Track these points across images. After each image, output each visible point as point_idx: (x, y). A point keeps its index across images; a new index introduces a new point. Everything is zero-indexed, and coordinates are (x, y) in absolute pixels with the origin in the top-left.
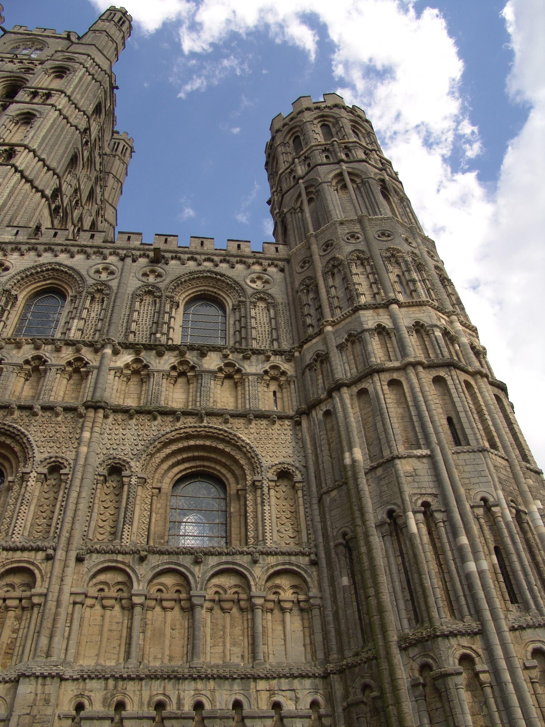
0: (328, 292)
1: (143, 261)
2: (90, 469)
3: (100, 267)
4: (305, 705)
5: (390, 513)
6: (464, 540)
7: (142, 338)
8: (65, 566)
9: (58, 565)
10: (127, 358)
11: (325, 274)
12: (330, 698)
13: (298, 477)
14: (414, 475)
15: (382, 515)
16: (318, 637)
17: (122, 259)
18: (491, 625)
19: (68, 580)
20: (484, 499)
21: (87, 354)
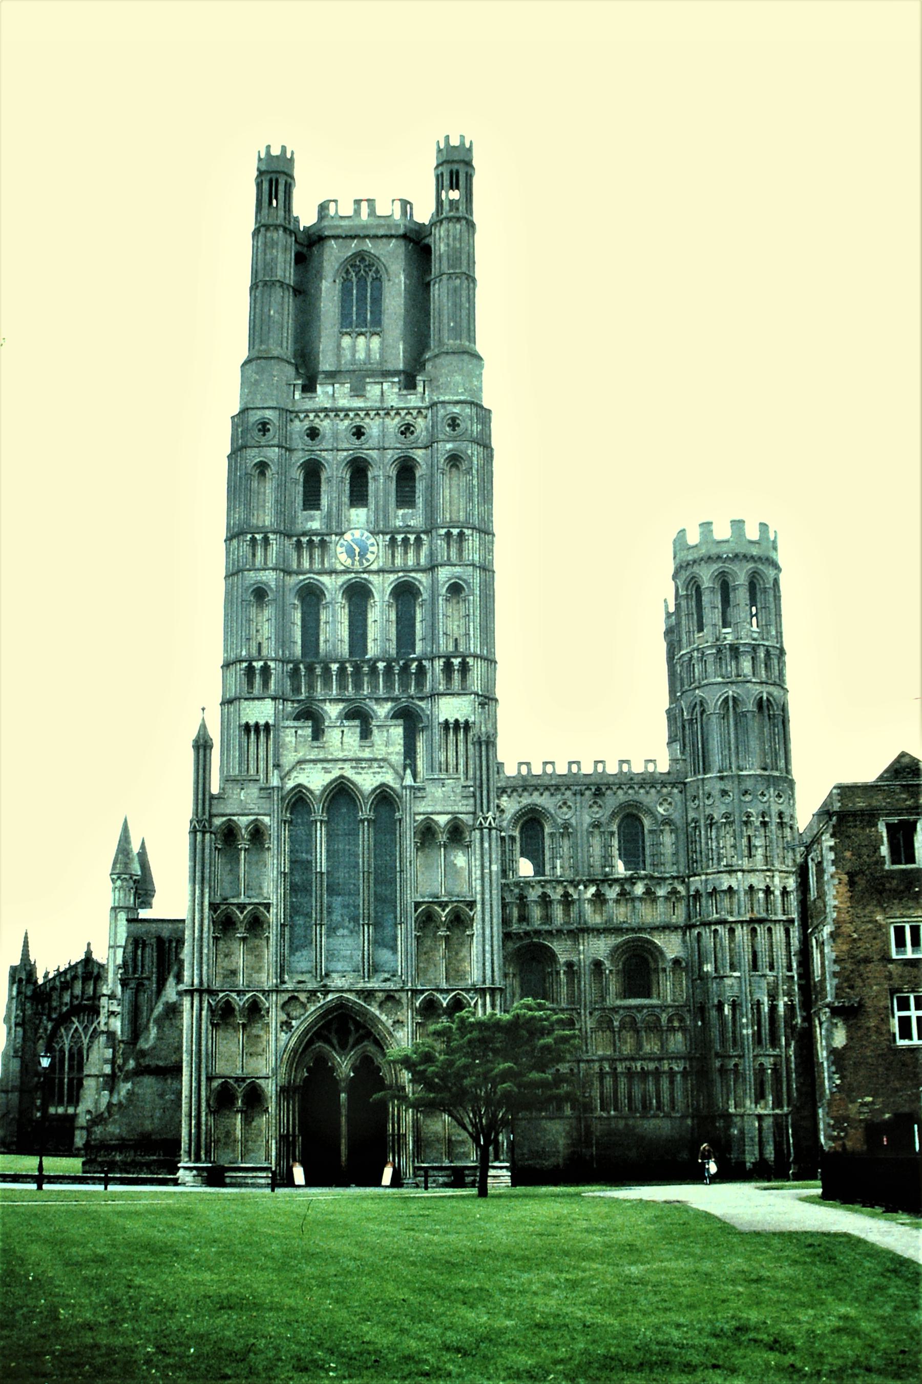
0: (707, 844)
1: (588, 793)
2: (587, 968)
3: (560, 803)
4: (681, 1069)
5: (719, 1001)
6: (744, 1020)
7: (598, 873)
8: (586, 1017)
9: (583, 1017)
10: (592, 890)
11: (706, 825)
12: (691, 1066)
13: (684, 964)
14: (732, 986)
15: (716, 1002)
16: (688, 1043)
17: (575, 794)
18: (746, 1056)
19: (588, 1023)
20: (758, 1001)
21: (571, 890)
